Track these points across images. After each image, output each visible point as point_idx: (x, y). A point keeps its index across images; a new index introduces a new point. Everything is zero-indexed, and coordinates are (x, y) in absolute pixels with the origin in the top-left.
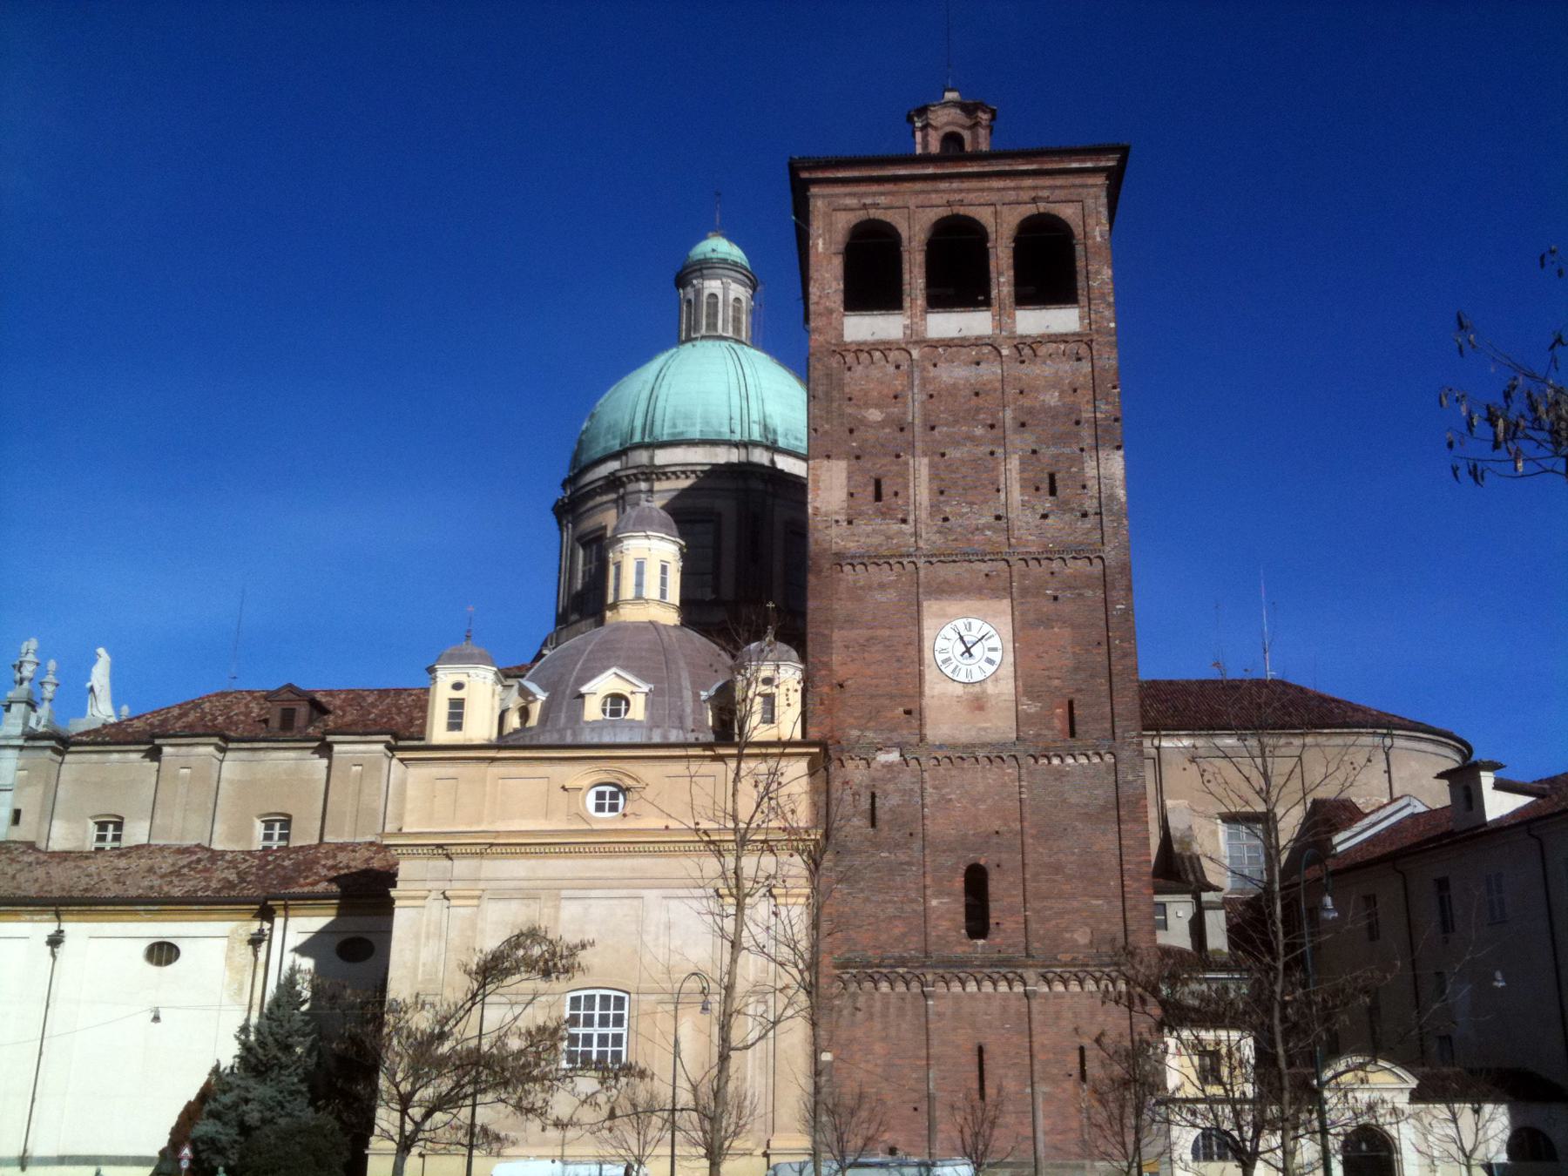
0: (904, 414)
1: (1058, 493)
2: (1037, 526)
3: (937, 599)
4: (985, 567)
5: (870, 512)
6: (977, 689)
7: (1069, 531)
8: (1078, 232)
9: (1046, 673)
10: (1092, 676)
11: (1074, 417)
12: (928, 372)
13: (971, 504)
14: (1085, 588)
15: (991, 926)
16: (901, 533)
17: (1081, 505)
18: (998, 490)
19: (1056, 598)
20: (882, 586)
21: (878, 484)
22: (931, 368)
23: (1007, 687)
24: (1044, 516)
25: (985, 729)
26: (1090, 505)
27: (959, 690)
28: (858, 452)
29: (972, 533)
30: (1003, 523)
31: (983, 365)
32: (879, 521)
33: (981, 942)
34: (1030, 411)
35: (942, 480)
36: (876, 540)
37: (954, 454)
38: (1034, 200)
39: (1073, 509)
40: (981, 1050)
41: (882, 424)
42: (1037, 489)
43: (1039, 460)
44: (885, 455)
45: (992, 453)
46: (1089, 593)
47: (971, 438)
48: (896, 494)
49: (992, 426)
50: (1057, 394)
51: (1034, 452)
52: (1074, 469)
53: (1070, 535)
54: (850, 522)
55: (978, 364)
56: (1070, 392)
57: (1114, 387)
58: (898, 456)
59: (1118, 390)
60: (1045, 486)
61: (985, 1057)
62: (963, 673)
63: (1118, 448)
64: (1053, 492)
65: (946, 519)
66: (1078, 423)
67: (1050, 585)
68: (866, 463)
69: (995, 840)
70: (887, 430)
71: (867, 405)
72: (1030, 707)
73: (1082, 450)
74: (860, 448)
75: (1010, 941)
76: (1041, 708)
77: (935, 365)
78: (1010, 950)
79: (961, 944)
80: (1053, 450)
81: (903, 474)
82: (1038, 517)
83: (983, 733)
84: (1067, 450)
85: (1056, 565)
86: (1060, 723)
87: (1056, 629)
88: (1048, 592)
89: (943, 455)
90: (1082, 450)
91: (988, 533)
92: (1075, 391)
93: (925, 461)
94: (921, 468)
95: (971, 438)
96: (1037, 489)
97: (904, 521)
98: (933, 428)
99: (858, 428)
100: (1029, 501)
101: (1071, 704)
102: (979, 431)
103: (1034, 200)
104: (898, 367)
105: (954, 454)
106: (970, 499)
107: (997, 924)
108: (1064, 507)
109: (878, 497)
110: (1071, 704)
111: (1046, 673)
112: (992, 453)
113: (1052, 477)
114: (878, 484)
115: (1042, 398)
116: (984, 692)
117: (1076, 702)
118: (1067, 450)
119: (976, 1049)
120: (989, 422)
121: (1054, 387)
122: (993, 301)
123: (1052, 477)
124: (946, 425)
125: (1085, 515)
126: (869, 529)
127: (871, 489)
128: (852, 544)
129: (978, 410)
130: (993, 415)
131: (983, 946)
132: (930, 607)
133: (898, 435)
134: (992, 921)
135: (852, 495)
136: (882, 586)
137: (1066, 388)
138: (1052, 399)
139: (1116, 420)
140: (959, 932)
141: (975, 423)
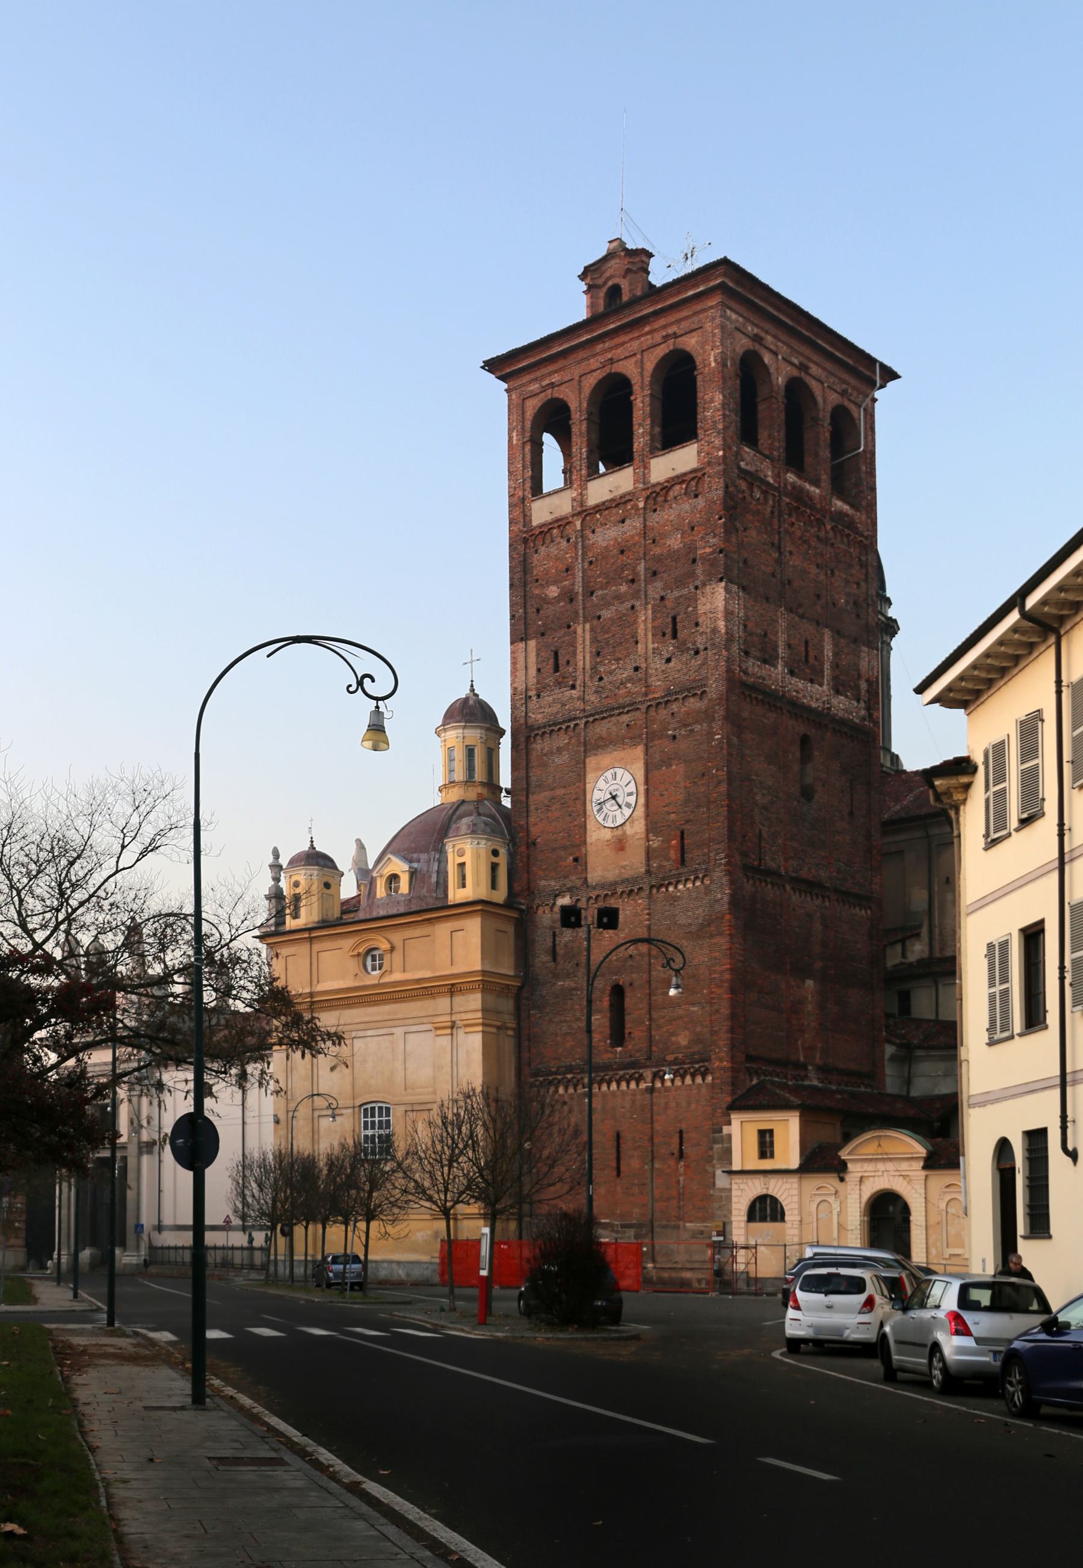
0: (573, 584)
1: (679, 635)
2: (663, 671)
3: (595, 755)
4: (625, 718)
5: (551, 684)
6: (619, 832)
7: (685, 671)
8: (698, 360)
9: (666, 809)
10: (698, 807)
11: (691, 556)
12: (589, 540)
13: (618, 660)
14: (695, 723)
15: (626, 1036)
16: (571, 698)
17: (694, 643)
18: (637, 642)
19: (674, 737)
20: (560, 750)
21: (556, 654)
22: (591, 536)
23: (638, 828)
24: (668, 660)
25: (624, 867)
26: (700, 644)
27: (607, 835)
28: (542, 629)
29: (618, 688)
30: (640, 675)
31: (627, 522)
32: (557, 691)
33: (619, 1049)
34: (659, 559)
35: (599, 641)
36: (554, 710)
37: (606, 614)
38: (666, 338)
39: (688, 648)
40: (618, 1136)
41: (558, 599)
42: (664, 634)
43: (665, 607)
44: (560, 628)
45: (633, 607)
46: (697, 728)
47: (619, 597)
48: (568, 662)
49: (633, 581)
50: (679, 536)
51: (662, 598)
52: (690, 609)
53: (685, 675)
54: (539, 696)
55: (623, 521)
56: (689, 531)
57: (720, 518)
58: (569, 627)
59: (723, 520)
60: (669, 631)
61: (621, 1141)
62: (610, 819)
63: (721, 580)
64: (675, 636)
65: (601, 679)
66: (694, 561)
67: (672, 726)
68: (548, 639)
69: (630, 963)
70: (562, 604)
71: (548, 584)
72: (655, 844)
73: (696, 588)
74: (544, 624)
75: (638, 1047)
76: (662, 841)
77: (593, 532)
78: (638, 1054)
79: (607, 1052)
80: (676, 593)
81: (573, 644)
82: (664, 661)
83: (623, 871)
84: (685, 591)
85: (674, 707)
86: (673, 854)
87: (674, 767)
88: (670, 732)
89: (599, 617)
90: (696, 588)
91: (629, 685)
92: (693, 529)
93: (588, 626)
94: (583, 632)
95: (619, 597)
96: (664, 634)
97: (573, 687)
98: (592, 594)
99: (542, 606)
100: (658, 648)
101: (682, 833)
102: (623, 588)
103: (666, 338)
104: (568, 541)
105: (606, 614)
106: (618, 655)
107: (630, 1033)
108: (682, 648)
109: (556, 669)
110: (682, 833)
111: (666, 809)
112: (633, 607)
113: (674, 619)
114: (556, 654)
115: (668, 543)
116: (624, 833)
117: (686, 832)
118: (685, 591)
119: (615, 1135)
120: (630, 577)
121: (678, 530)
122: (636, 455)
123: (674, 619)
124: (601, 588)
125: (697, 653)
126: (551, 698)
127: (552, 661)
128: (540, 716)
129: (623, 567)
130: (634, 569)
131: (620, 1052)
132: (591, 762)
133: (569, 606)
134: (627, 1031)
135: (539, 670)
136: (560, 750)
137: (686, 528)
138: (675, 542)
139: (721, 552)
140: (605, 1042)
141: (620, 581)
